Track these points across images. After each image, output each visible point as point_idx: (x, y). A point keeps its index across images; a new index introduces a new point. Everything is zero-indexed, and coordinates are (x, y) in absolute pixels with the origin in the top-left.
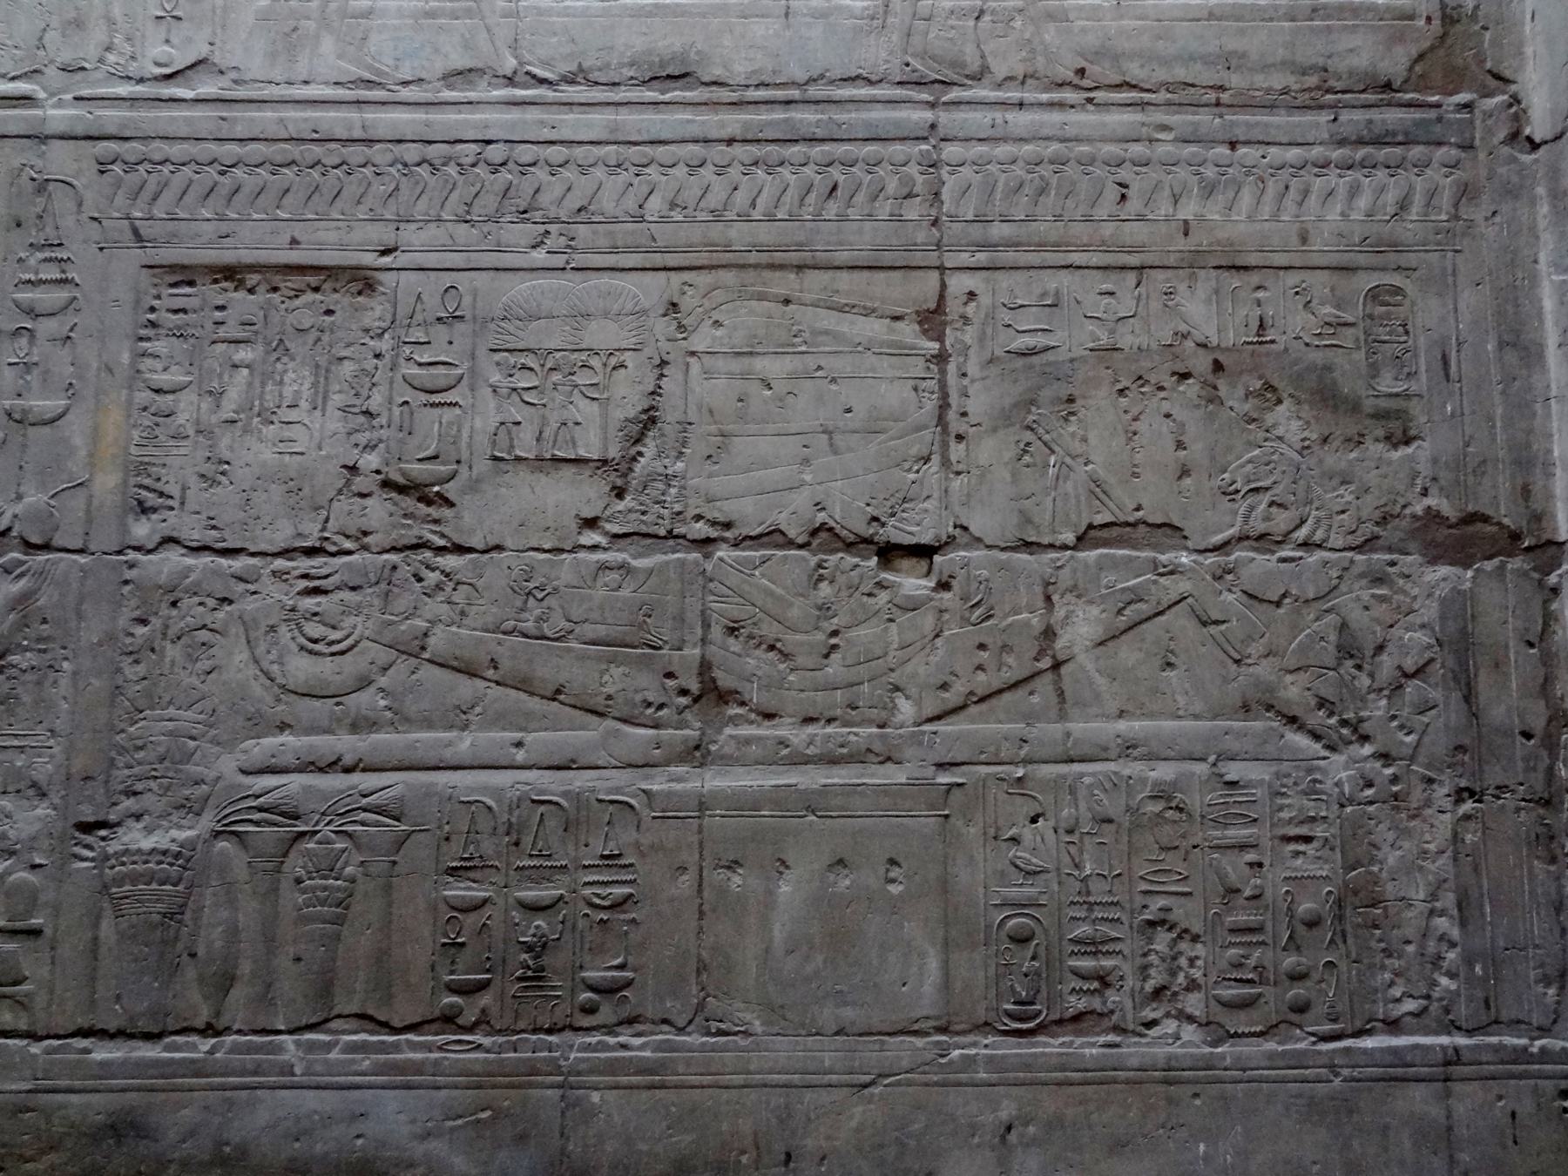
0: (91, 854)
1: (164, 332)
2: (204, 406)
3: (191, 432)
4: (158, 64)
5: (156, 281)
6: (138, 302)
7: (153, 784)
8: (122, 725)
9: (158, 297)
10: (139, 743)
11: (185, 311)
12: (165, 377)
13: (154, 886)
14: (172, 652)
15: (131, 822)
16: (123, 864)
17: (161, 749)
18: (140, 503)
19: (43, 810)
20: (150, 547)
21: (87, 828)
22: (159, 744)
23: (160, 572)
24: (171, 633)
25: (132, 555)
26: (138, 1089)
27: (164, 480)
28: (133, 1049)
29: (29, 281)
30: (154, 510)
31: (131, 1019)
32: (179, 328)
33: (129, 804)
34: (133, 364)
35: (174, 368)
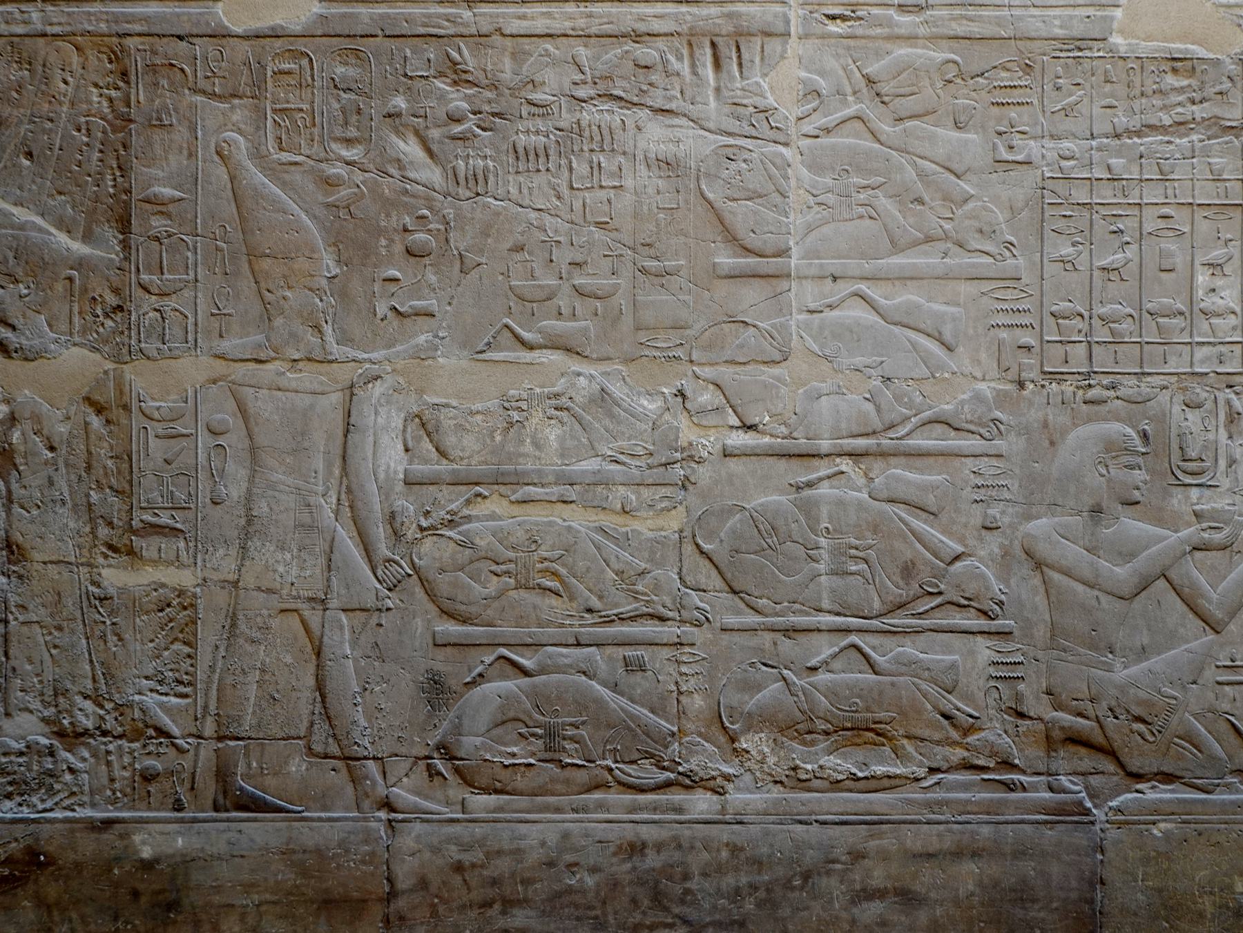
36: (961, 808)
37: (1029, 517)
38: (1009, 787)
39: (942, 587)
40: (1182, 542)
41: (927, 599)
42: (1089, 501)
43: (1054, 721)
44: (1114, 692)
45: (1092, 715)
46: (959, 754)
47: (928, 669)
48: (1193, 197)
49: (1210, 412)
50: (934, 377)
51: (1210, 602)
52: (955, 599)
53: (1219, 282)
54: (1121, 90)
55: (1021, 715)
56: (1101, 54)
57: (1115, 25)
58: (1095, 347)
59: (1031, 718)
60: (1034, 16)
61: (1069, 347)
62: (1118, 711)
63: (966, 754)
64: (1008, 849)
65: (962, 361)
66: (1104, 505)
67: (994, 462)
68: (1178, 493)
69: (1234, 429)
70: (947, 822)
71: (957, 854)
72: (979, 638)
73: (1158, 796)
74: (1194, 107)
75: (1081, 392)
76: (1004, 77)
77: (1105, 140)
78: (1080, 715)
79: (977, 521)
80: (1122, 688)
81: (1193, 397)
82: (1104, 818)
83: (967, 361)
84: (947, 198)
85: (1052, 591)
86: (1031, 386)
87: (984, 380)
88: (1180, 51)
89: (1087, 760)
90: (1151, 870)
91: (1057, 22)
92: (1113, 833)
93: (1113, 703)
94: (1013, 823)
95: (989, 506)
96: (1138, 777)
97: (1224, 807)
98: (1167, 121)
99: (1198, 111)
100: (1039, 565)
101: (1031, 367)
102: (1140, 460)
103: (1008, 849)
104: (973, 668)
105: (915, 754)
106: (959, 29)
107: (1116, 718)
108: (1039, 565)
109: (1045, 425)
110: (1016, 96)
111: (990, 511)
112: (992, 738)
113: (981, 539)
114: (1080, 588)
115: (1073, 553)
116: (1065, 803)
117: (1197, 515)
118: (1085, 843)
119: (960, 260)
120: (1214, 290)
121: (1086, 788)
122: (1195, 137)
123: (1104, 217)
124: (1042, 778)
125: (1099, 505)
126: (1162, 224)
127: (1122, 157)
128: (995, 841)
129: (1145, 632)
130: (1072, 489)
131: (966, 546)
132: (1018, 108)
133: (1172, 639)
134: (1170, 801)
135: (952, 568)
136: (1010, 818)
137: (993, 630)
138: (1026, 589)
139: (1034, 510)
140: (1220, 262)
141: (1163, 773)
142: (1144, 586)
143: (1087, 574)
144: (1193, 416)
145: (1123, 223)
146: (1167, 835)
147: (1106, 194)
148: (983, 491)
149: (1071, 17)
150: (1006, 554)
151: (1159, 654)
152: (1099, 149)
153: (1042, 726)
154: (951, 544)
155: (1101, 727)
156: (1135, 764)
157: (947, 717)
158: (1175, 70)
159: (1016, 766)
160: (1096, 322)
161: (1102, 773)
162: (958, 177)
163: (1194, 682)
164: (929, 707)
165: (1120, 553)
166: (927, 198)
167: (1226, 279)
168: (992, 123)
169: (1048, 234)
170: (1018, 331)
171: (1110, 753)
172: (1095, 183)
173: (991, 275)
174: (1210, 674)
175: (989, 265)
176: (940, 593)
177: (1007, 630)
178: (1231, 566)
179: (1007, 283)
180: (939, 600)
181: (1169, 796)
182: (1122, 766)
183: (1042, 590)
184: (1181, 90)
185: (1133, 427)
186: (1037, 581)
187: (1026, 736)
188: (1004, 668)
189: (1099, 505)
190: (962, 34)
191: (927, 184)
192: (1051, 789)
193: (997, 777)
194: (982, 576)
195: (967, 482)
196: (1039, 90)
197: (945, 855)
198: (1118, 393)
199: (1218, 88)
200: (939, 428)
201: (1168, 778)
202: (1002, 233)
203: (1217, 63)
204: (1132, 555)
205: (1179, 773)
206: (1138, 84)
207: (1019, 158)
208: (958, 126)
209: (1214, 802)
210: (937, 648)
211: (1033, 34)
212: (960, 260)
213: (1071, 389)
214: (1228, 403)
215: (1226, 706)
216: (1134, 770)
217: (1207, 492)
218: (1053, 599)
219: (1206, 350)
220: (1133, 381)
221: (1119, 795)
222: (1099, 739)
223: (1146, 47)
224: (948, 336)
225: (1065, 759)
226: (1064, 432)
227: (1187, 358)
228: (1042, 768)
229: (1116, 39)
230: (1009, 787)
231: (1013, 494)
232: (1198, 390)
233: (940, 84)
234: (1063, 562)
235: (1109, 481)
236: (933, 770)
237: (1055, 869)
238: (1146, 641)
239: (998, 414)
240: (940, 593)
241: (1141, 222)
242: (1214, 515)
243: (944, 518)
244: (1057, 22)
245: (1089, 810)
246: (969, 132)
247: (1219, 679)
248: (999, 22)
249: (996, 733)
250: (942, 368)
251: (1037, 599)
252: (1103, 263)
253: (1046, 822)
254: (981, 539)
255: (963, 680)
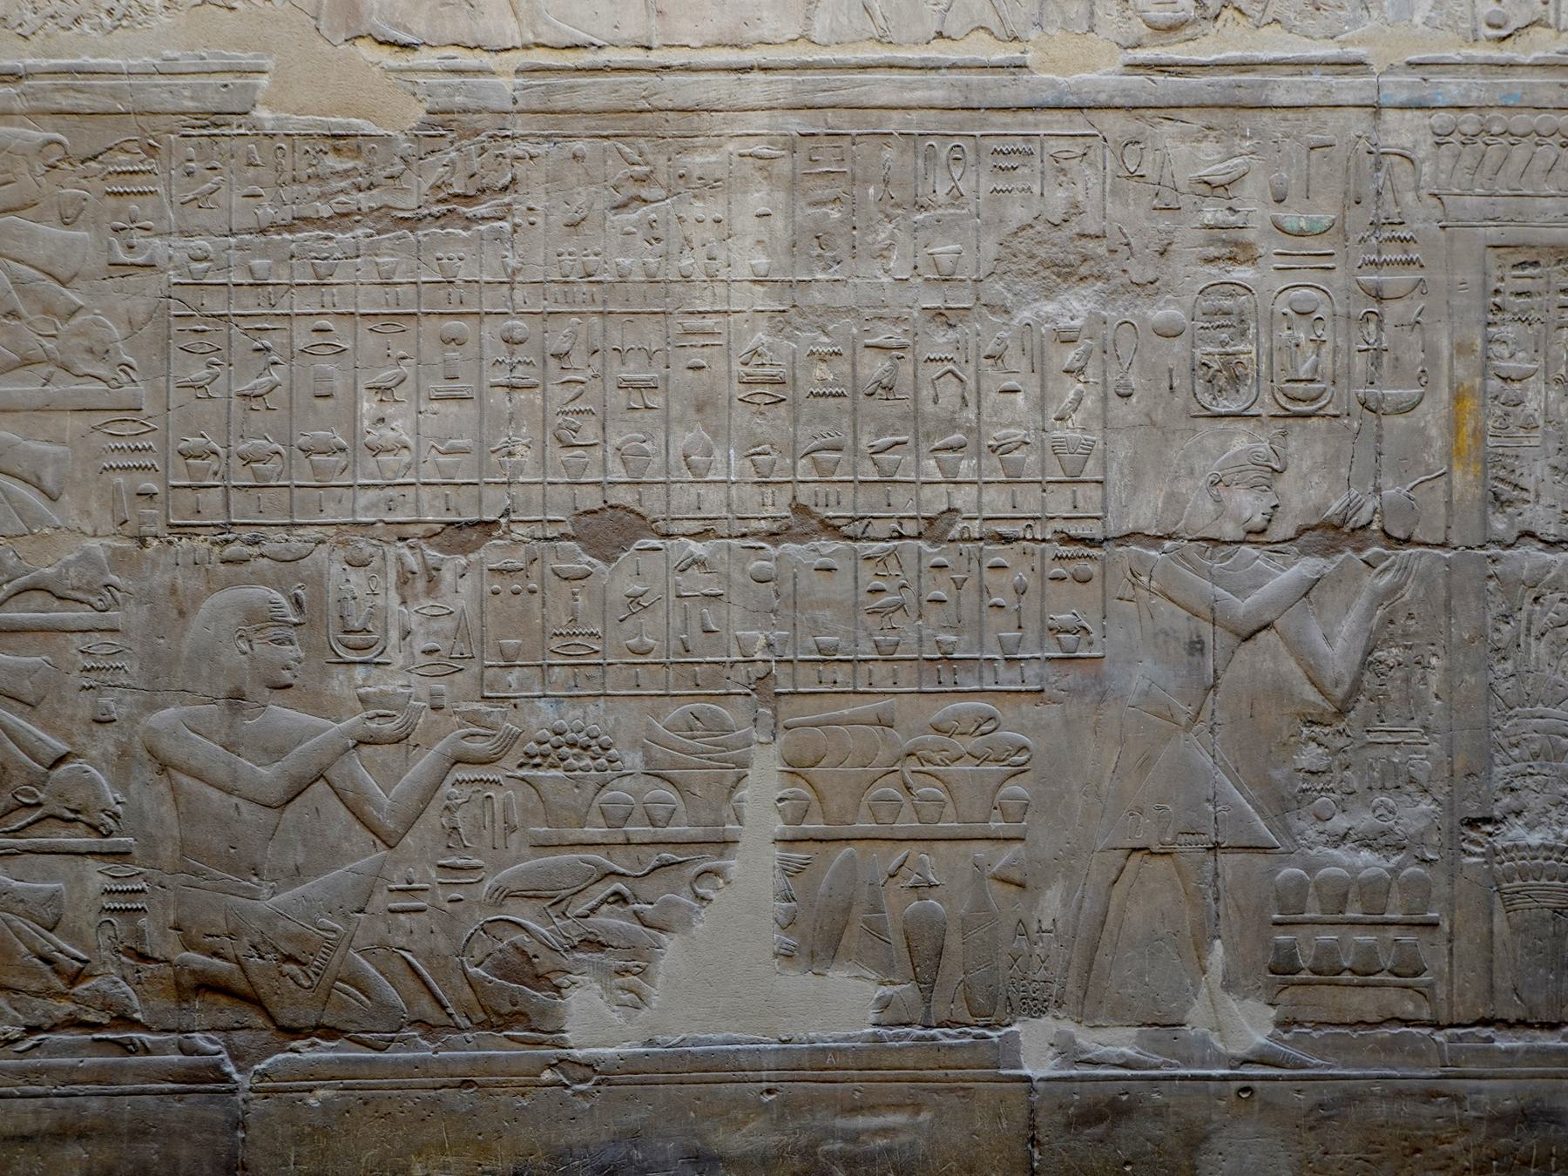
0: (1479, 850)
1: (1508, 316)
2: (1552, 395)
3: (1541, 423)
4: (1491, 25)
5: (1500, 262)
6: (1485, 283)
7: (1529, 780)
8: (1498, 722)
9: (1502, 279)
10: (1514, 740)
11: (1527, 294)
12: (1512, 364)
13: (1544, 881)
14: (1539, 649)
15: (1512, 818)
16: (1512, 859)
17: (1536, 747)
18: (1496, 496)
19: (1426, 805)
20: (1510, 541)
21: (1473, 823)
22: (1533, 740)
23: (1522, 568)
24: (1534, 631)
25: (1494, 551)
26: (1543, 1076)
27: (1518, 472)
28: (1535, 1038)
29: (1373, 263)
30: (1510, 503)
31: (1531, 1010)
32: (1523, 311)
33: (1507, 800)
34: (1486, 349)
35: (1521, 355)
36: (65, 1078)
37: (152, 707)
38: (126, 1048)
39: (42, 796)
40: (344, 734)
41: (23, 812)
42: (224, 685)
43: (184, 964)
44: (257, 925)
45: (231, 955)
46: (66, 1007)
47: (22, 901)
48: (356, 305)
49: (378, 571)
50: (32, 534)
51: (380, 809)
52: (57, 812)
53: (390, 410)
54: (268, 175)
55: (144, 957)
56: (242, 131)
57: (259, 95)
58: (233, 492)
59: (156, 961)
60: (157, 86)
61: (201, 494)
62: (263, 948)
63: (72, 1007)
64: (123, 1128)
65: (69, 511)
66: (246, 689)
67: (108, 638)
68: (340, 673)
69: (407, 590)
70: (47, 1095)
71: (60, 1135)
72: (90, 861)
73: (316, 1055)
74: (361, 195)
75: (217, 549)
76: (122, 161)
77: (248, 237)
78: (215, 954)
79: (85, 712)
80: (269, 919)
81: (355, 553)
82: (247, 1086)
83: (73, 513)
84: (48, 310)
85: (181, 799)
86: (156, 543)
87: (95, 536)
88: (341, 126)
89: (229, 1013)
90: (305, 1151)
91: (187, 93)
92: (259, 1104)
93: (257, 939)
94: (130, 1094)
95: (100, 695)
96: (294, 1032)
97: (397, 1068)
98: (325, 211)
99: (364, 200)
100: (164, 767)
101: (153, 519)
102: (292, 633)
103: (123, 1128)
104: (82, 898)
105: (9, 1009)
106: (65, 102)
107: (261, 957)
108: (164, 767)
109: (173, 591)
110: (138, 184)
111: (101, 700)
112: (105, 987)
113: (91, 735)
114: (215, 794)
115: (205, 751)
116: (198, 1068)
117: (363, 700)
118: (222, 1117)
119: (66, 386)
120: (383, 420)
121: (228, 1047)
122: (359, 232)
123: (246, 331)
124: (172, 1036)
125: (238, 689)
126: (317, 339)
127: (268, 257)
128: (107, 1117)
129: (300, 848)
130: (205, 672)
131: (73, 744)
132: (139, 198)
133: (334, 856)
134: (329, 1062)
135: (55, 773)
136: (128, 1088)
137: (105, 850)
138: (151, 799)
139: (159, 698)
140: (389, 384)
141: (324, 1026)
142: (297, 791)
143: (221, 774)
144: (356, 577)
145: (269, 339)
146: (325, 1102)
147: (249, 303)
148: (93, 675)
149: (204, 86)
150: (124, 753)
151: (317, 876)
152: (239, 248)
153: (170, 971)
154: (53, 742)
155: (243, 971)
156: (286, 1016)
157: (47, 960)
158: (337, 150)
159: (137, 1022)
160: (236, 463)
161: (249, 1027)
162: (63, 284)
163: (361, 911)
164: (23, 949)
165: (265, 750)
166: (23, 310)
167: (397, 405)
168: (107, 218)
169: (175, 352)
170: (138, 475)
171: (254, 1001)
172: (233, 289)
173: (103, 406)
174: (381, 900)
175: (100, 393)
176: (39, 805)
177: (122, 849)
178: (407, 762)
179: (124, 415)
180: (38, 813)
181: (331, 1054)
182: (272, 1019)
183: (169, 798)
184: (345, 174)
185: (283, 592)
186: (163, 787)
187: (151, 984)
188: (121, 897)
189: (238, 689)
190: (69, 109)
191: (24, 294)
192: (183, 1051)
193: (110, 1036)
194: (93, 782)
195: (74, 664)
196: (166, 175)
197: (43, 1137)
198: (264, 550)
199: (388, 172)
200: (38, 598)
201: (331, 1033)
202: (118, 353)
203: (387, 140)
204: (282, 752)
205: (341, 1026)
206: (289, 168)
207: (139, 260)
208: (66, 222)
209: (385, 1062)
210: (36, 874)
211: (157, 108)
212: (66, 386)
213: (207, 545)
214: (400, 558)
215: (401, 940)
216: (286, 1022)
217: (376, 672)
218: (182, 809)
219: (372, 494)
220: (282, 534)
221: (270, 1055)
222: (241, 985)
223: (298, 122)
224: (49, 482)
225: (201, 1011)
226: (197, 600)
227: (347, 504)
228: (171, 1023)
229: (263, 113)
230: (126, 1048)
231: (131, 677)
232: (361, 545)
233: (40, 169)
234: (192, 762)
235: (253, 659)
236: (31, 1030)
237: (184, 1152)
238: (300, 860)
239: (113, 578)
240: (39, 805)
241: (291, 337)
242: (383, 699)
243: (44, 709)
244: (187, 93)
245: (229, 1075)
246: (78, 229)
247: (392, 905)
248: (115, 93)
249: (111, 981)
250: (41, 521)
251: (163, 809)
252: (244, 388)
253: (173, 1092)
254: (91, 735)
255: (68, 915)
